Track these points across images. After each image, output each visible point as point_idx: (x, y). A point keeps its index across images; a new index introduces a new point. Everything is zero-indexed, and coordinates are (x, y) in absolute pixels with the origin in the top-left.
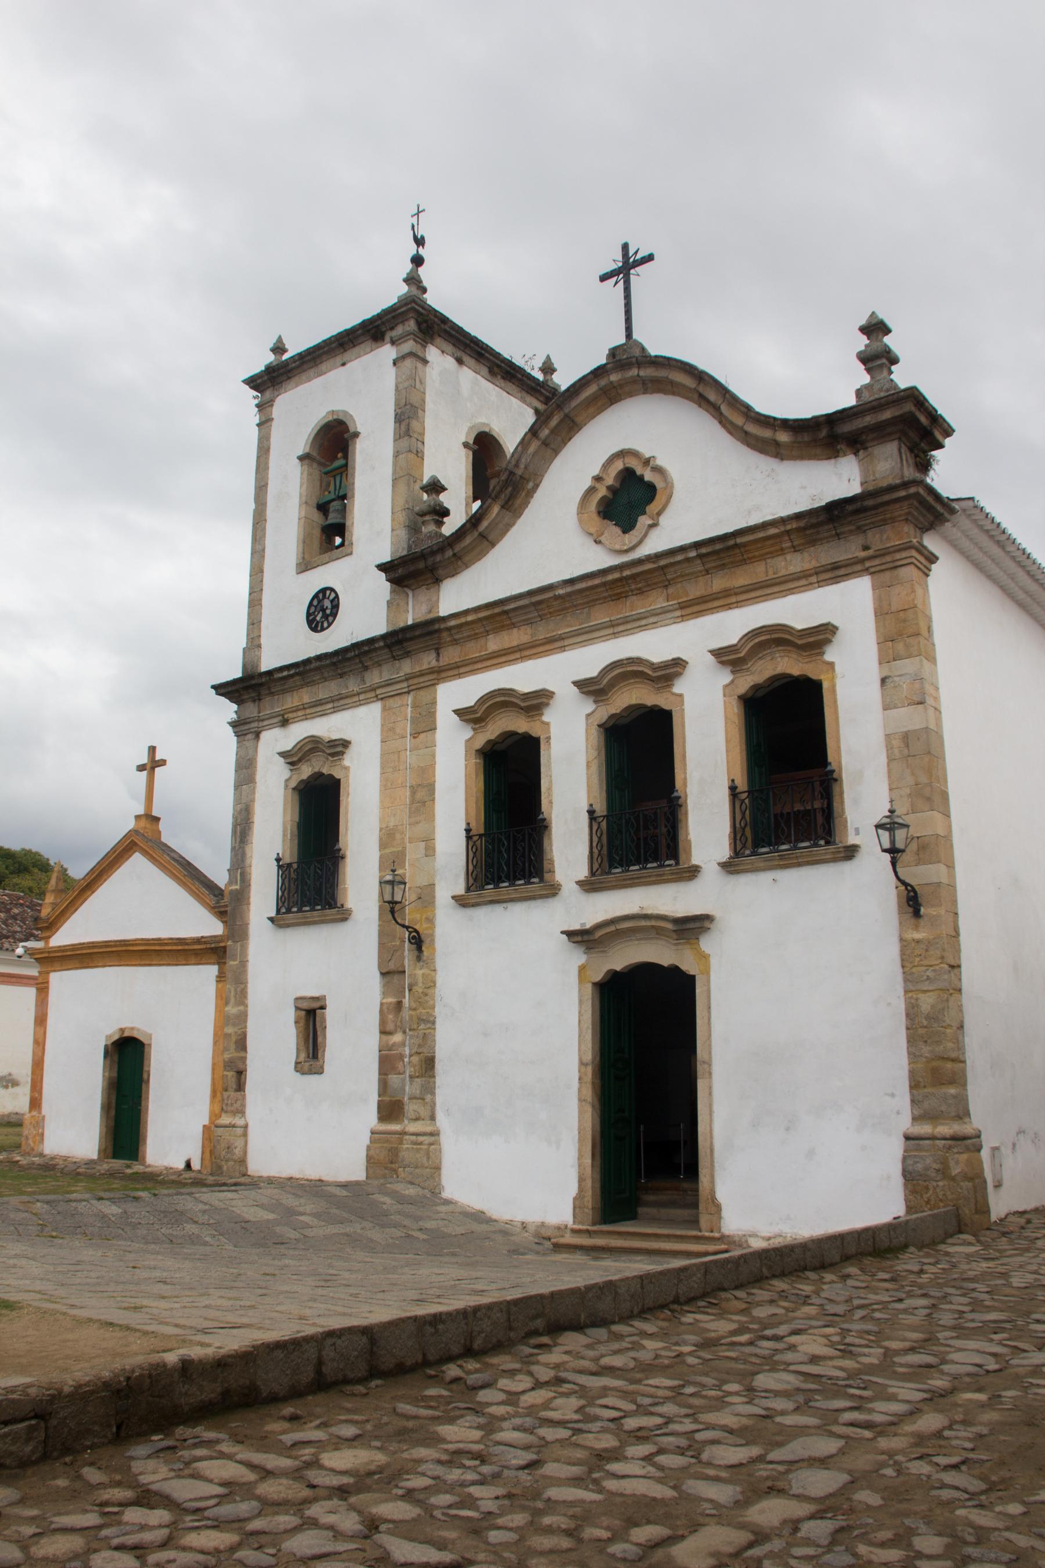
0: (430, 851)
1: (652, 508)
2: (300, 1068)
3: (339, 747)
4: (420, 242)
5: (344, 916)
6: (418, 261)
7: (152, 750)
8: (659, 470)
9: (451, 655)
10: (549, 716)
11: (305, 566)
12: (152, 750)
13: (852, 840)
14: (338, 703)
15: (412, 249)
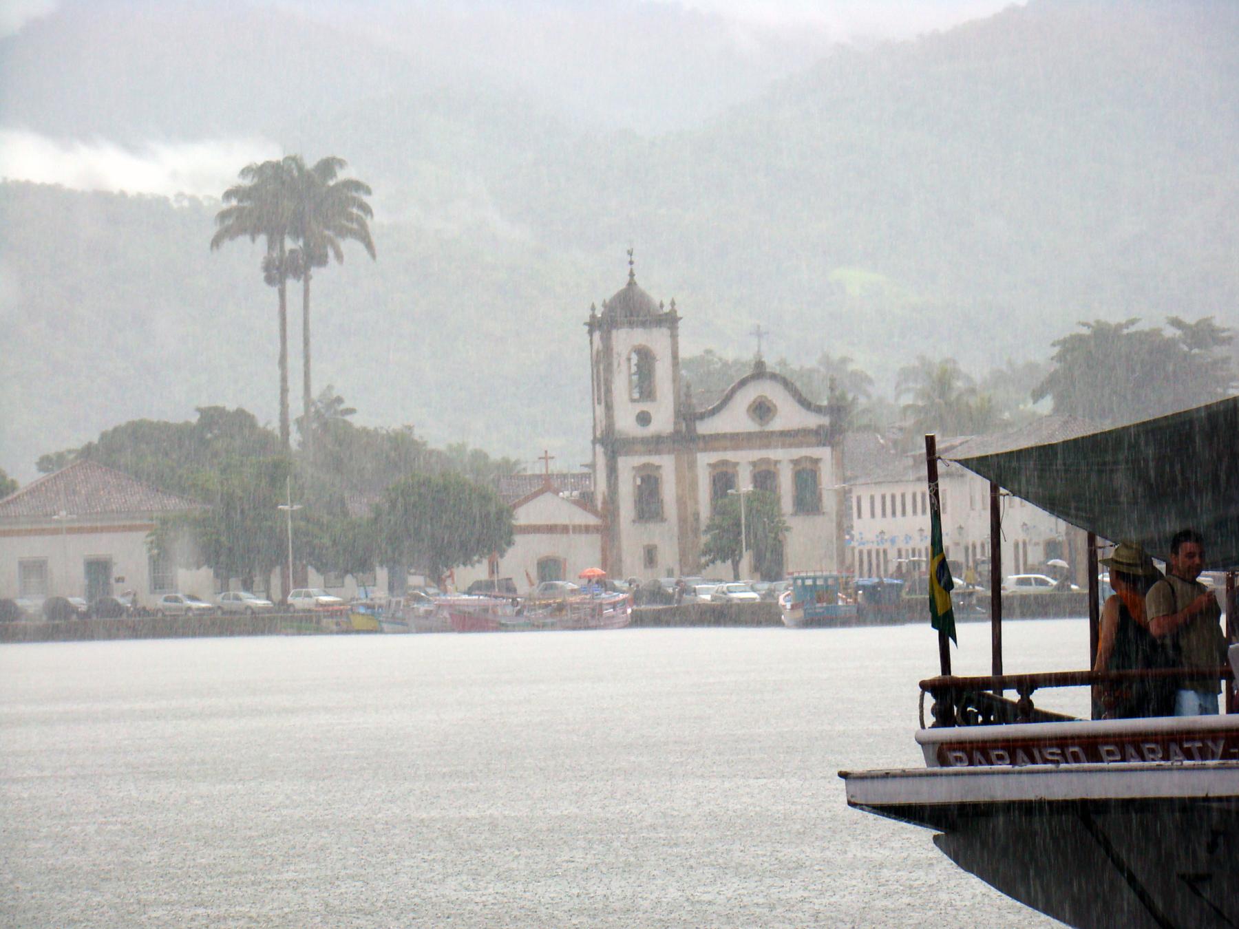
0: (696, 502)
1: (771, 414)
2: (645, 566)
3: (659, 467)
4: (630, 253)
5: (663, 520)
6: (631, 263)
7: (546, 452)
8: (775, 406)
9: (701, 445)
10: (738, 468)
11: (633, 401)
12: (546, 452)
13: (825, 510)
14: (658, 452)
15: (634, 258)
